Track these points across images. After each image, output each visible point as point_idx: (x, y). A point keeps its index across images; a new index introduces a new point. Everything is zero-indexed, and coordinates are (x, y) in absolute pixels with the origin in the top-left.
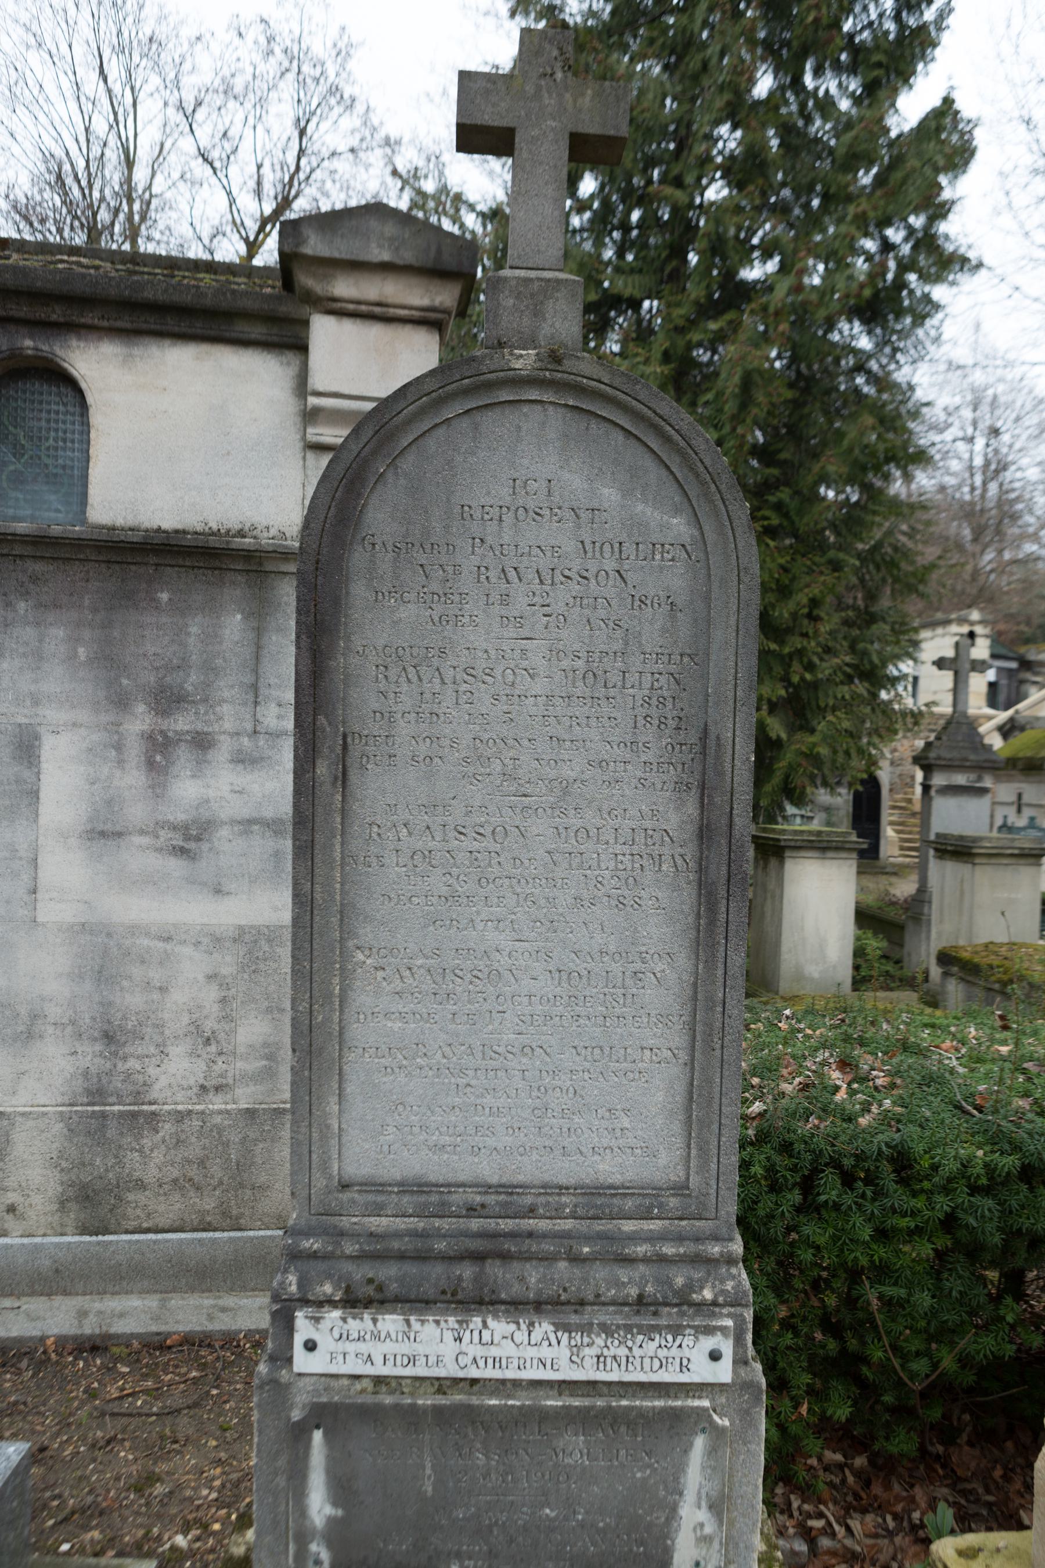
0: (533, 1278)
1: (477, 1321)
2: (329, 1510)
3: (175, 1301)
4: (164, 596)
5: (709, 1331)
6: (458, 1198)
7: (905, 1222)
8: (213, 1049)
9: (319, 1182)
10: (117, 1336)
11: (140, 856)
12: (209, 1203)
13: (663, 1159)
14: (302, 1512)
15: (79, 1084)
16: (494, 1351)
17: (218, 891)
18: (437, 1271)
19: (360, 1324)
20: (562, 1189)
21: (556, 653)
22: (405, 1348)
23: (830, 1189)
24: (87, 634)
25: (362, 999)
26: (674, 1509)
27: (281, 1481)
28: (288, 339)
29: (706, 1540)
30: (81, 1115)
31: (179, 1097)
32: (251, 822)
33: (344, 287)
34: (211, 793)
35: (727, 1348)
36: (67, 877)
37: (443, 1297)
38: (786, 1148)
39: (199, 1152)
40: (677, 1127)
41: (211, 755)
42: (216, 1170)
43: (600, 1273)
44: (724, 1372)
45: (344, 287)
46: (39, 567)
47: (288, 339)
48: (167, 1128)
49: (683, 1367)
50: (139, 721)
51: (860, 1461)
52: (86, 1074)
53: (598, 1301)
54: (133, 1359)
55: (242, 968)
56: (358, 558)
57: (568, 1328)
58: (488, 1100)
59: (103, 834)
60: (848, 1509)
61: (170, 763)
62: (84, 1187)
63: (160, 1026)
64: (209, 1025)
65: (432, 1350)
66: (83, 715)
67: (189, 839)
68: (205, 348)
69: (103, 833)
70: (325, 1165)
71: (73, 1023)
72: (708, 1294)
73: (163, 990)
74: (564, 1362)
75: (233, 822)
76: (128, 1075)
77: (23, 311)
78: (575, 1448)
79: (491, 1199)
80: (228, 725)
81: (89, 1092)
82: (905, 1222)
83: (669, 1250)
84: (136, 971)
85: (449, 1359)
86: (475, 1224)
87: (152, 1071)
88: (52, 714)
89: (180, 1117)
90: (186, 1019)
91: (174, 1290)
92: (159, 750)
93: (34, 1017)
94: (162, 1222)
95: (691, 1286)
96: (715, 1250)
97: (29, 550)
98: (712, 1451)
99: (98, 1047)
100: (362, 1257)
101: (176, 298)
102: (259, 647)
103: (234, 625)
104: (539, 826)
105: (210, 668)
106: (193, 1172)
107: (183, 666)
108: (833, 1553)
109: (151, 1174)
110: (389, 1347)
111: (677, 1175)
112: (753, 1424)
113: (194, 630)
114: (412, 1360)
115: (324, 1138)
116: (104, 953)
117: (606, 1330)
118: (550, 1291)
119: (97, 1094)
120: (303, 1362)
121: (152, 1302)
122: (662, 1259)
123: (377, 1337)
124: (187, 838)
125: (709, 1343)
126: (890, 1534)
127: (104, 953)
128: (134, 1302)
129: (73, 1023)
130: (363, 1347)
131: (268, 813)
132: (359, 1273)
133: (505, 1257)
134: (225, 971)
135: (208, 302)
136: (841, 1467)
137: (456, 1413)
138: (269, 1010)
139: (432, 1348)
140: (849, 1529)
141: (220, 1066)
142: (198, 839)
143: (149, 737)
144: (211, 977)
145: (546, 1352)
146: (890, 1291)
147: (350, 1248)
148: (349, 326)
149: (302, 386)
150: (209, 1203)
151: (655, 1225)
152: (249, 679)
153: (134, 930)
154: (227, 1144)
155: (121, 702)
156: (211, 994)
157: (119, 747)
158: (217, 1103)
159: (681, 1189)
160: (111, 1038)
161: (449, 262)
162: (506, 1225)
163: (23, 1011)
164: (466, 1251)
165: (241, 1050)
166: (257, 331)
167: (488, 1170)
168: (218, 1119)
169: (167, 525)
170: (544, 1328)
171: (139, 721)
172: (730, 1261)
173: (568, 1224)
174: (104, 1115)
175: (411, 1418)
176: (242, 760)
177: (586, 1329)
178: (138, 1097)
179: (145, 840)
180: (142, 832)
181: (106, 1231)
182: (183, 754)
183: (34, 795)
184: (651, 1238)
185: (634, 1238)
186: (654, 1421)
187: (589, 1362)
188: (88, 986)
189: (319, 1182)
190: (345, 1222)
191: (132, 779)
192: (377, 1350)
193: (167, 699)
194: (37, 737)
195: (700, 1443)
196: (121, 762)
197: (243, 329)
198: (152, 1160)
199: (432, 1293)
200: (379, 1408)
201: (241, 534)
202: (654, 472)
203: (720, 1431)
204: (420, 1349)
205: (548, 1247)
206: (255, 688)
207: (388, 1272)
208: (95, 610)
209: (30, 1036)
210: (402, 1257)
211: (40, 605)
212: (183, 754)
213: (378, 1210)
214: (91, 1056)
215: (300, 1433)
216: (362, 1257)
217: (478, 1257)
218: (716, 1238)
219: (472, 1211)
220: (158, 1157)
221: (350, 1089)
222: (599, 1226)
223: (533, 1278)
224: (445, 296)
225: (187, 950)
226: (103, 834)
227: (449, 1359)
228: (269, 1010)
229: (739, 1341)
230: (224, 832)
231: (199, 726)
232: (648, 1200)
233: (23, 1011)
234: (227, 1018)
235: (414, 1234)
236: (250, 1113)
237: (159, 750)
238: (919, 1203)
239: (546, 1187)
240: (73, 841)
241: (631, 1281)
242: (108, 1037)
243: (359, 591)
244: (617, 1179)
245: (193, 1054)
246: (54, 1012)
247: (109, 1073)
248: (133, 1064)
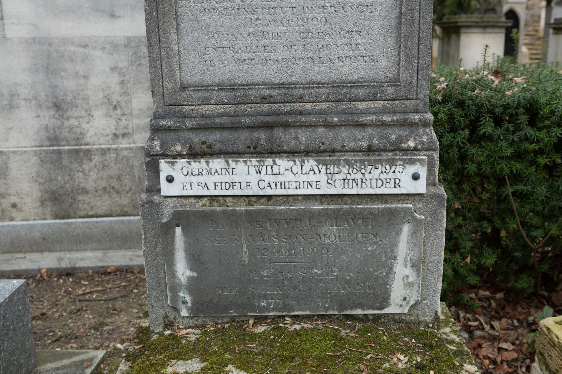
0: (304, 137)
1: (269, 161)
2: (188, 273)
3: (111, 253)
5: (412, 162)
6: (254, 93)
7: (533, 146)
8: (119, 112)
9: (169, 85)
10: (80, 269)
12: (125, 201)
13: (383, 64)
14: (173, 275)
16: (280, 178)
17: (113, 15)
18: (244, 136)
20: (319, 85)
22: (227, 178)
23: (488, 128)
26: (391, 267)
27: (160, 260)
29: (411, 284)
30: (47, 152)
31: (102, 140)
35: (423, 172)
37: (249, 150)
38: (461, 104)
39: (117, 172)
40: (392, 42)
42: (127, 182)
43: (344, 134)
44: (421, 187)
48: (97, 159)
49: (397, 184)
51: (499, 295)
52: (47, 128)
53: (344, 150)
54: (90, 278)
55: (132, 63)
57: (325, 163)
58: (271, 29)
60: (492, 318)
62: (53, 192)
63: (86, 99)
64: (115, 98)
65: (243, 179)
70: (171, 74)
71: (35, 98)
72: (411, 144)
73: (86, 77)
74: (323, 183)
76: (71, 129)
78: (331, 233)
79: (276, 92)
81: (49, 139)
82: (533, 146)
83: (387, 118)
84: (69, 66)
85: (254, 185)
86: (266, 108)
87: (84, 126)
89: (104, 152)
90: (101, 95)
91: (110, 248)
93: (13, 95)
94: (100, 212)
95: (400, 139)
96: (416, 117)
98: (414, 234)
99: (52, 112)
100: (198, 129)
106: (114, 183)
108: (483, 338)
109: (90, 185)
110: (217, 178)
111: (391, 73)
112: (438, 219)
114: (231, 185)
115: (169, 57)
116: (49, 57)
117: (349, 163)
118: (314, 145)
119: (54, 140)
120: (166, 189)
121: (99, 254)
122: (383, 124)
123: (209, 172)
125: (411, 169)
126: (515, 328)
127: (49, 57)
128: (89, 254)
129: (35, 98)
130: (201, 179)
132: (197, 138)
133: (286, 126)
134: (122, 65)
136: (488, 299)
137: (260, 214)
139: (245, 177)
140: (492, 327)
141: (124, 122)
144: (114, 69)
145: (312, 178)
146: (520, 187)
147: (190, 123)
150: (125, 201)
151: (378, 104)
153: (65, 41)
154: (132, 167)
156: (115, 79)
158: (124, 144)
159: (395, 82)
162: (286, 107)
163: (5, 92)
164: (261, 122)
165: (135, 112)
168: (125, 153)
170: (311, 163)
172: (425, 124)
173: (324, 106)
174: (59, 152)
175: (233, 218)
177: (336, 163)
178: (78, 141)
181: (69, 217)
184: (376, 112)
185: (365, 112)
186: (377, 215)
187: (339, 183)
189: (169, 85)
190: (186, 109)
192: (210, 180)
195: (406, 229)
198: (90, 177)
199: (241, 147)
200: (213, 213)
203: (419, 222)
204: (236, 179)
205: (312, 119)
207: (215, 137)
209: (11, 107)
210: (222, 128)
214: (48, 118)
215: (167, 230)
216: (198, 129)
217: (269, 127)
218: (416, 112)
219: (264, 99)
220: (93, 175)
221: (183, 25)
222: (343, 106)
223: (304, 137)
227: (254, 185)
229: (430, 171)
232: (373, 89)
233: (5, 92)
234: (125, 93)
235: (229, 115)
238: (542, 134)
239: (310, 85)
241: (363, 138)
242: (57, 106)
244: (354, 77)
245: (108, 115)
246: (24, 92)
247: (60, 128)
248: (73, 122)
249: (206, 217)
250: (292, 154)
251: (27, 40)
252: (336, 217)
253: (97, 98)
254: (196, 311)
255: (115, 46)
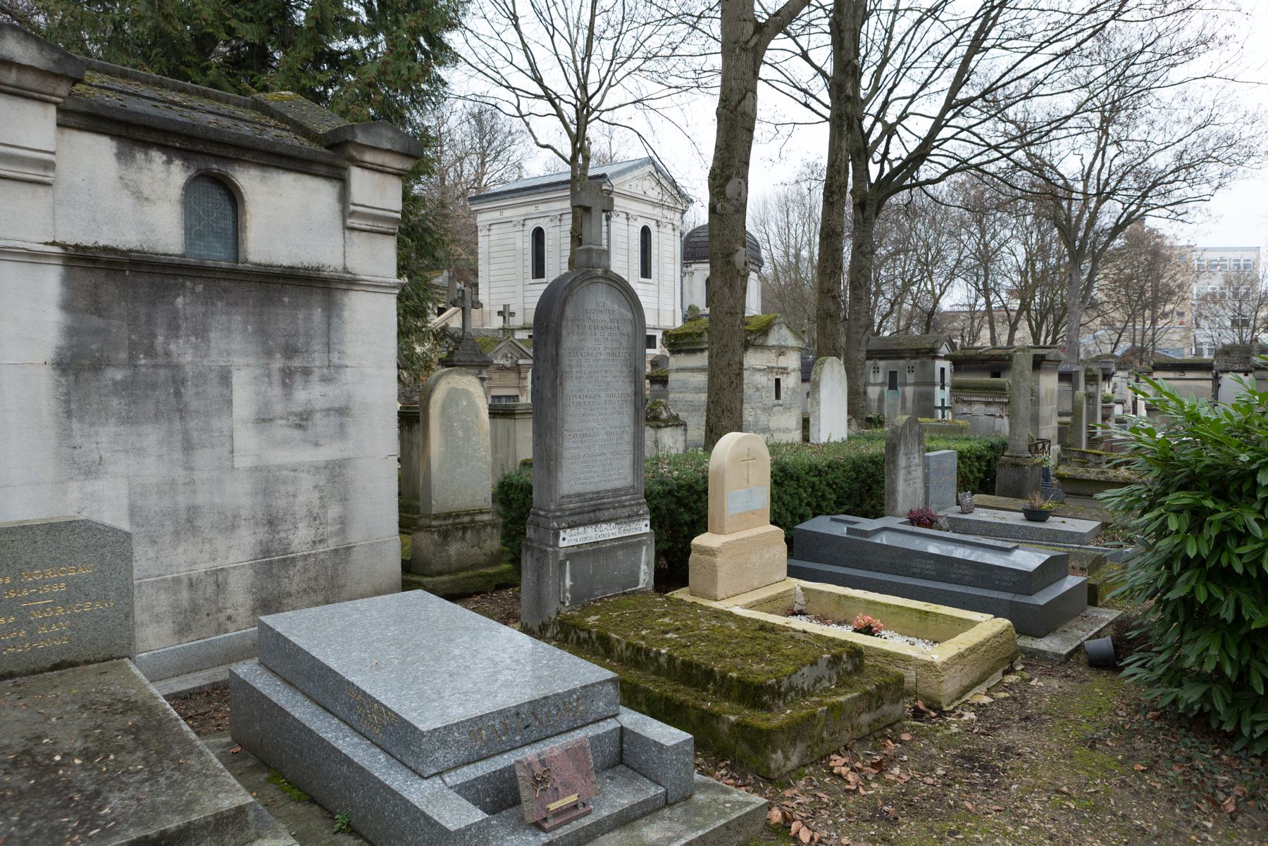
4: (286, 300)
11: (281, 430)
15: (258, 548)
17: (317, 445)
18: (586, 516)
19: (574, 531)
21: (606, 348)
24: (251, 319)
25: (566, 444)
28: (338, 176)
32: (329, 410)
33: (369, 157)
34: (312, 397)
36: (248, 444)
41: (311, 378)
42: (322, 582)
43: (619, 511)
45: (369, 157)
46: (227, 284)
47: (338, 176)
48: (300, 564)
50: (278, 363)
52: (261, 543)
55: (329, 481)
56: (564, 323)
59: (264, 420)
61: (293, 383)
64: (315, 511)
66: (252, 360)
67: (303, 420)
68: (298, 176)
69: (263, 420)
73: (294, 496)
75: (322, 410)
76: (280, 540)
77: (215, 151)
80: (317, 363)
84: (282, 488)
87: (291, 537)
88: (237, 360)
89: (305, 558)
92: (288, 376)
93: (235, 517)
97: (223, 275)
101: (291, 152)
102: (329, 324)
103: (318, 314)
104: (603, 394)
105: (308, 336)
106: (312, 584)
107: (296, 335)
113: (300, 316)
116: (267, 481)
119: (266, 552)
124: (302, 420)
127: (267, 481)
129: (253, 517)
131: (337, 405)
135: (305, 155)
137: (596, 550)
138: (341, 500)
141: (321, 530)
142: (307, 420)
143: (283, 370)
144: (315, 487)
148: (367, 174)
149: (344, 196)
152: (325, 340)
153: (280, 467)
155: (269, 353)
156: (317, 495)
157: (269, 376)
159: (633, 487)
160: (272, 523)
161: (413, 151)
166: (323, 170)
167: (593, 488)
168: (322, 556)
169: (285, 264)
171: (278, 363)
174: (271, 562)
175: (587, 553)
176: (325, 380)
178: (285, 551)
179: (283, 422)
180: (281, 418)
182: (298, 378)
183: (230, 402)
188: (260, 498)
191: (276, 391)
192: (578, 537)
193: (290, 351)
194: (230, 372)
196: (270, 383)
197: (316, 168)
201: (318, 269)
202: (624, 301)
206: (328, 344)
207: (576, 518)
208: (255, 307)
211: (228, 304)
212: (298, 378)
213: (571, 502)
214: (262, 533)
215: (562, 564)
217: (594, 511)
219: (592, 499)
220: (297, 579)
223: (606, 514)
224: (407, 165)
225: (304, 475)
226: (264, 420)
228: (341, 500)
230: (318, 415)
231: (305, 364)
232: (626, 491)
234: (323, 506)
236: (336, 551)
237: (288, 376)
240: (250, 425)
241: (626, 512)
242: (271, 523)
243: (564, 332)
246: (245, 513)
247: (272, 541)
248: (282, 535)
249: (578, 554)
250: (604, 522)
251: (250, 469)
252: (622, 547)
253: (302, 512)
254: (573, 602)
255: (317, 468)
